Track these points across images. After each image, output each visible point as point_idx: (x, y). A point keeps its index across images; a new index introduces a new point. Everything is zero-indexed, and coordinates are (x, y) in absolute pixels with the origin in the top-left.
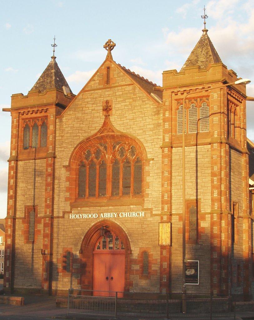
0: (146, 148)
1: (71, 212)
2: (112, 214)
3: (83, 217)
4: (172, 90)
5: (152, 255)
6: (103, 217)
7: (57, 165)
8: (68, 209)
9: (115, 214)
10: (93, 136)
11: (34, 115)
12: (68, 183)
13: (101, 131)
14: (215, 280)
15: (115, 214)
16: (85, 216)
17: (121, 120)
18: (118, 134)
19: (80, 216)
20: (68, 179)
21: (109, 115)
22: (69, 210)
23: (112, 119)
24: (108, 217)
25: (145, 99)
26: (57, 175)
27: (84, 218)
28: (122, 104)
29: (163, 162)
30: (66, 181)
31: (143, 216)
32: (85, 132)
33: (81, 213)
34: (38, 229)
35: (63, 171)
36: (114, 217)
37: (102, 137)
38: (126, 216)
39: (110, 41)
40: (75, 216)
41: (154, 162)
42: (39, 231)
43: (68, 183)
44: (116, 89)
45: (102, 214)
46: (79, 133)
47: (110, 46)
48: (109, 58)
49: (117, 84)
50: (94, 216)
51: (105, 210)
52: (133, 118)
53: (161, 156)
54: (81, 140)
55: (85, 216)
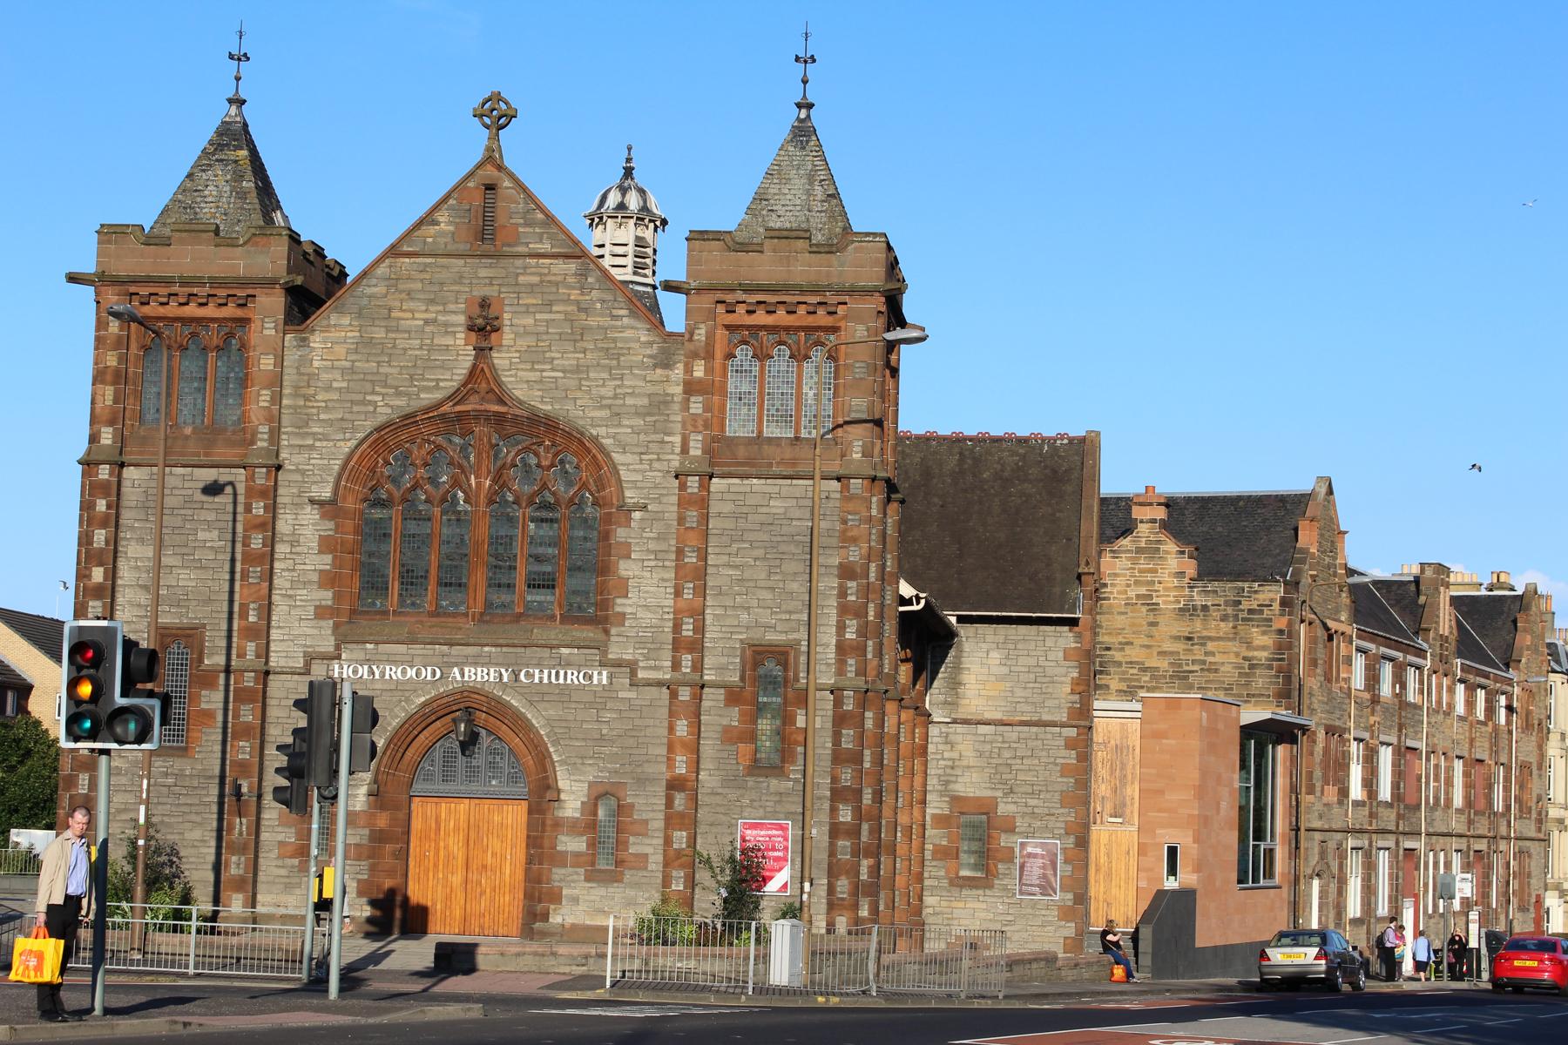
0: (620, 467)
1: (339, 657)
2: (492, 670)
3: (383, 674)
4: (719, 296)
6: (459, 678)
7: (285, 495)
9: (503, 671)
11: (192, 310)
12: (328, 558)
13: (457, 396)
14: (843, 885)
15: (503, 671)
16: (394, 673)
17: (532, 369)
18: (518, 412)
20: (326, 545)
21: (491, 349)
22: (332, 649)
23: (500, 359)
24: (479, 679)
26: (283, 526)
27: (387, 677)
28: (538, 316)
29: (681, 520)
30: (320, 552)
31: (605, 682)
32: (398, 394)
33: (379, 662)
34: (204, 706)
35: (310, 515)
36: (501, 679)
37: (461, 417)
38: (546, 681)
39: (496, 97)
40: (355, 672)
41: (647, 515)
42: (209, 714)
43: (328, 558)
44: (519, 262)
45: (456, 670)
46: (373, 393)
47: (496, 114)
48: (492, 158)
49: (521, 249)
50: (427, 674)
51: (466, 657)
52: (578, 366)
53: (674, 499)
54: (381, 420)
55: (394, 673)
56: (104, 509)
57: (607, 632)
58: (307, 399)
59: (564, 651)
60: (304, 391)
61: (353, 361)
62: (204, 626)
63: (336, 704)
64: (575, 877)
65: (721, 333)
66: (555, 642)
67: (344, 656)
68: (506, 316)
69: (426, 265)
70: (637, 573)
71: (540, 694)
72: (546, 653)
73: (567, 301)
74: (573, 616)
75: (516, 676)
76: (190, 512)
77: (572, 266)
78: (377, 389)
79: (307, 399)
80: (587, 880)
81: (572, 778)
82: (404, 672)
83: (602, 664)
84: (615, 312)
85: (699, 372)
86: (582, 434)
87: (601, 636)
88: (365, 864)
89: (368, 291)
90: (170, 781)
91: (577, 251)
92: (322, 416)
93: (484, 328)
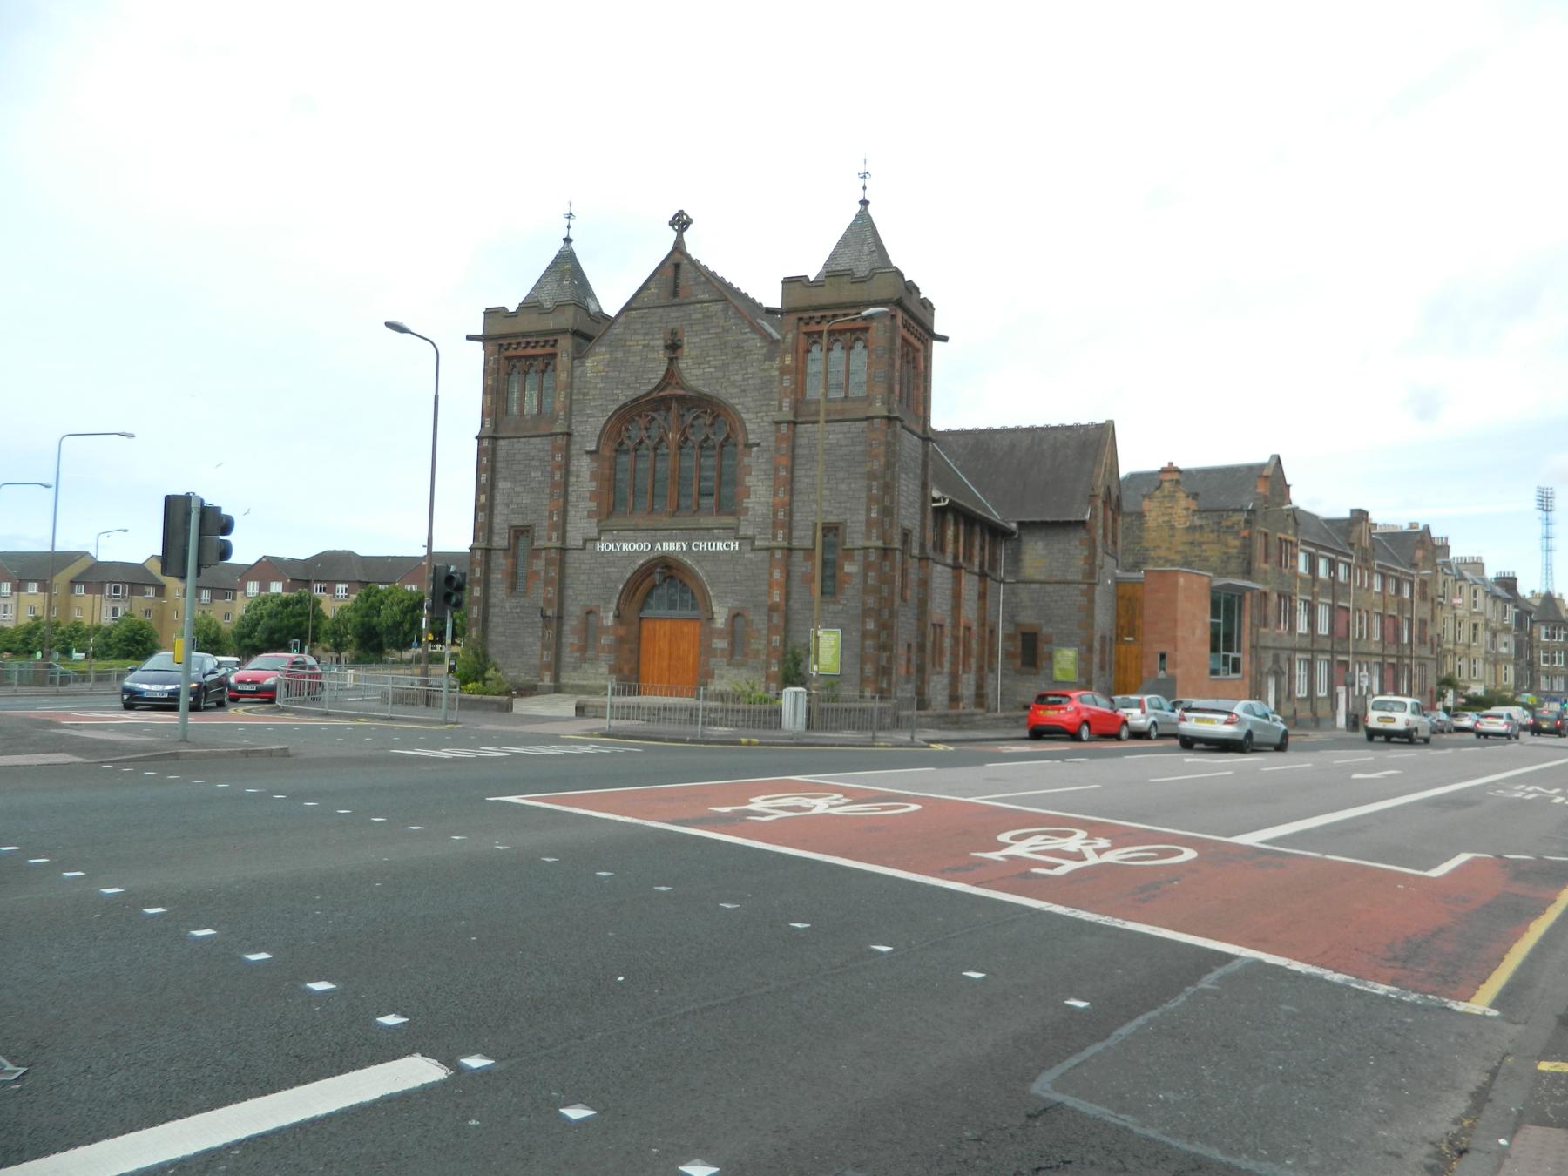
1: (599, 539)
3: (621, 548)
4: (800, 315)
5: (752, 621)
6: (660, 549)
7: (575, 448)
8: (594, 533)
10: (644, 396)
11: (530, 351)
12: (594, 484)
13: (658, 387)
14: (869, 668)
16: (626, 547)
17: (699, 368)
18: (691, 394)
19: (615, 547)
20: (593, 476)
21: (676, 358)
22: (596, 534)
23: (682, 364)
25: (746, 330)
26: (573, 468)
28: (702, 337)
29: (777, 449)
30: (591, 481)
31: (737, 548)
33: (619, 541)
35: (586, 460)
37: (663, 399)
38: (705, 549)
39: (681, 213)
41: (760, 449)
42: (536, 573)
43: (594, 484)
44: (692, 307)
45: (658, 544)
46: (618, 388)
48: (679, 247)
49: (693, 299)
50: (643, 547)
52: (723, 364)
53: (773, 439)
54: (621, 403)
55: (626, 547)
56: (485, 462)
57: (739, 519)
58: (584, 395)
59: (716, 531)
60: (582, 391)
61: (607, 372)
62: (535, 524)
63: (188, 514)
64: (721, 663)
65: (802, 337)
66: (710, 526)
67: (602, 538)
68: (685, 339)
69: (645, 313)
70: (755, 484)
71: (703, 556)
72: (706, 532)
73: (717, 326)
74: (720, 509)
75: (689, 546)
76: (527, 462)
77: (720, 306)
78: (620, 386)
79: (584, 395)
80: (728, 665)
81: (721, 605)
82: (632, 546)
83: (736, 539)
84: (743, 331)
85: (788, 361)
86: (725, 403)
87: (735, 521)
88: (612, 657)
89: (616, 331)
90: (518, 610)
91: (723, 298)
92: (592, 404)
93: (674, 347)
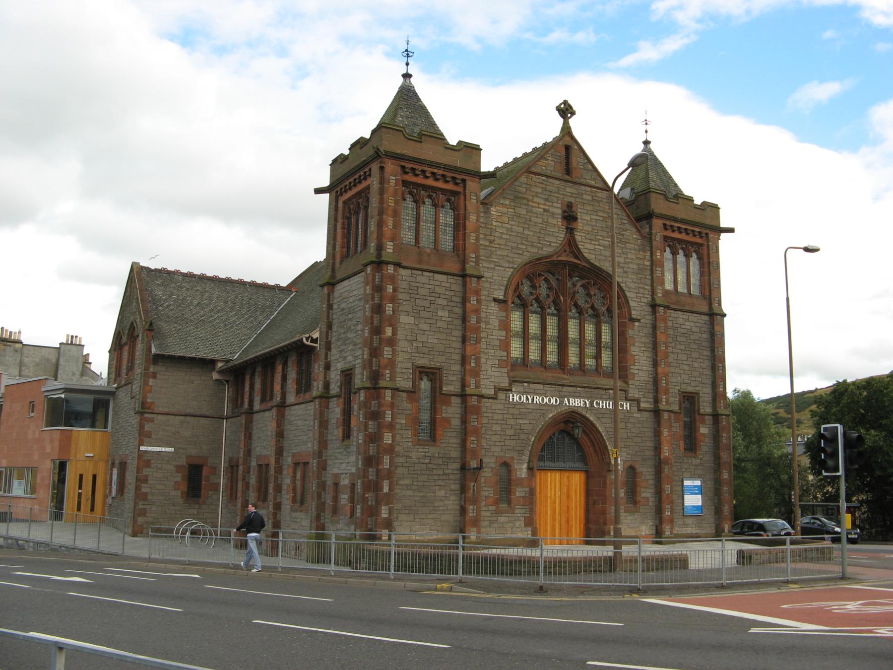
0: (629, 299)
1: (511, 390)
2: (582, 400)
6: (568, 404)
8: (505, 383)
9: (586, 401)
10: (546, 258)
11: (430, 182)
15: (586, 401)
16: (538, 399)
17: (591, 243)
19: (527, 399)
22: (507, 385)
24: (576, 405)
25: (625, 222)
27: (535, 402)
28: (592, 217)
31: (628, 409)
32: (532, 246)
34: (444, 415)
36: (586, 406)
38: (604, 407)
40: (520, 398)
41: (641, 324)
42: (447, 421)
45: (566, 399)
46: (522, 244)
47: (566, 111)
48: (566, 131)
51: (570, 392)
55: (538, 399)
61: (512, 225)
72: (603, 392)
76: (433, 299)
82: (543, 400)
90: (427, 461)
91: (600, 185)
93: (569, 217)
